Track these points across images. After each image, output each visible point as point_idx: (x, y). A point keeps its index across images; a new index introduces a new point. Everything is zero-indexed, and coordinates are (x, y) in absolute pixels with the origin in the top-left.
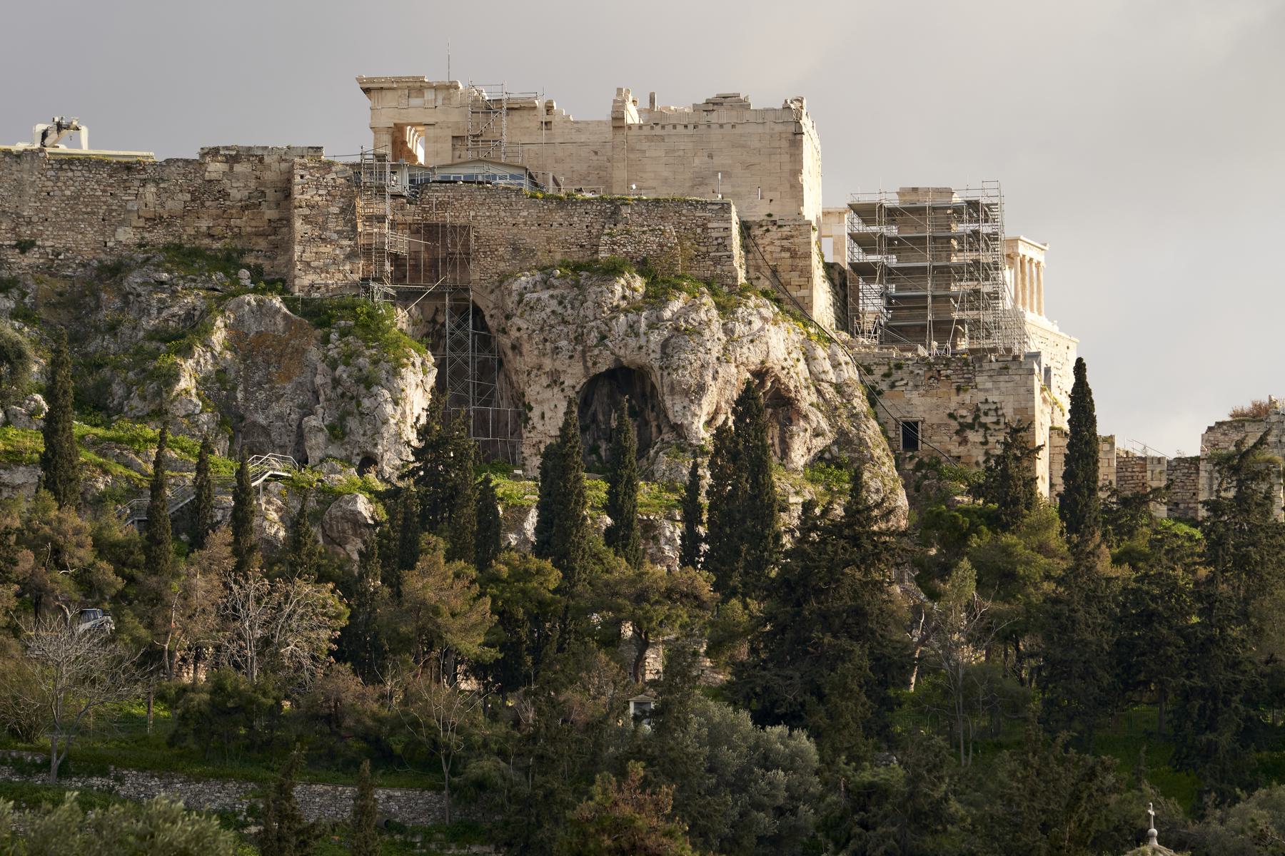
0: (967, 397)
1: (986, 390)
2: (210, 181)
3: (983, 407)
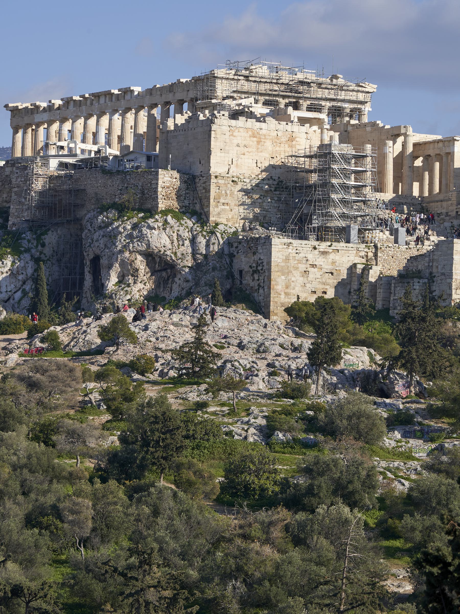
0: (255, 257)
1: (260, 253)
2: (7, 176)
3: (259, 262)
